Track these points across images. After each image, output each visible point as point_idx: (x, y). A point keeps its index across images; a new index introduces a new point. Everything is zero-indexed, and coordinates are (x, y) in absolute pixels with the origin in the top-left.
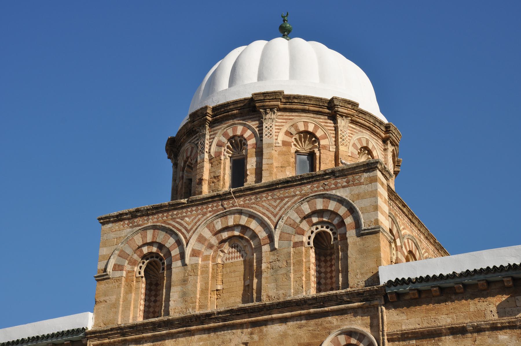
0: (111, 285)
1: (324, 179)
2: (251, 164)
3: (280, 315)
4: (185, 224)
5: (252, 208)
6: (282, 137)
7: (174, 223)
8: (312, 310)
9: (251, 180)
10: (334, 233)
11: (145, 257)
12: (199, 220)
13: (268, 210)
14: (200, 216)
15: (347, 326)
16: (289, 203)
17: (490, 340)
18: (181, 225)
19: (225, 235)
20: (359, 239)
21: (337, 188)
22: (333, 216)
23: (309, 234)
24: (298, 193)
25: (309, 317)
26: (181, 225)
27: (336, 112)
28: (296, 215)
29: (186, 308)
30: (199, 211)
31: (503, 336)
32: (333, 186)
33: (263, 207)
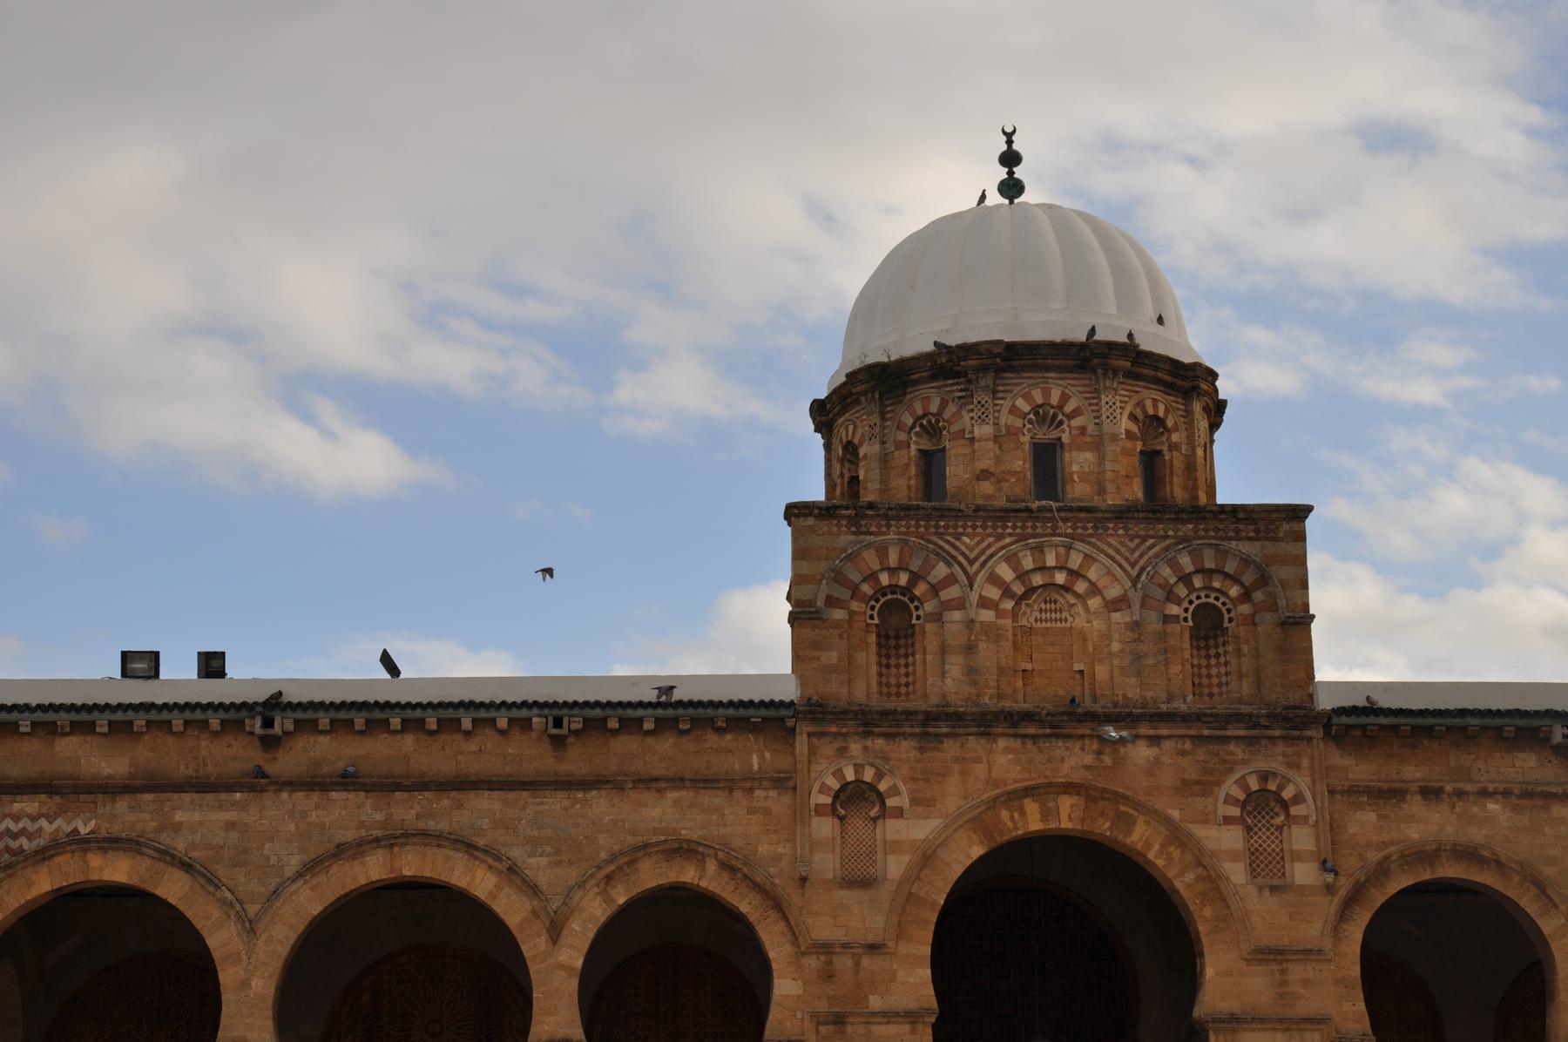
0: (824, 632)
1: (1215, 518)
2: (1078, 462)
3: (1152, 732)
4: (963, 548)
5: (1089, 543)
6: (1125, 424)
7: (941, 543)
8: (1206, 732)
9: (1078, 491)
10: (1229, 611)
11: (882, 591)
12: (989, 546)
13: (1118, 551)
14: (991, 540)
15: (1261, 764)
16: (1156, 549)
17: (1475, 810)
18: (956, 548)
19: (1037, 580)
20: (1278, 630)
21: (1240, 539)
22: (1228, 582)
23: (1186, 604)
24: (1171, 533)
25: (1199, 739)
26: (956, 548)
27: (1195, 388)
28: (1169, 570)
29: (978, 695)
30: (989, 530)
31: (1493, 806)
32: (1232, 534)
33: (1110, 545)
